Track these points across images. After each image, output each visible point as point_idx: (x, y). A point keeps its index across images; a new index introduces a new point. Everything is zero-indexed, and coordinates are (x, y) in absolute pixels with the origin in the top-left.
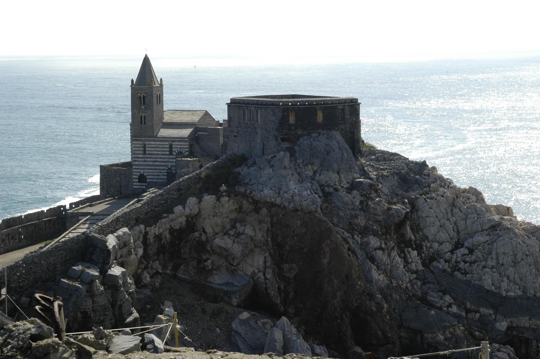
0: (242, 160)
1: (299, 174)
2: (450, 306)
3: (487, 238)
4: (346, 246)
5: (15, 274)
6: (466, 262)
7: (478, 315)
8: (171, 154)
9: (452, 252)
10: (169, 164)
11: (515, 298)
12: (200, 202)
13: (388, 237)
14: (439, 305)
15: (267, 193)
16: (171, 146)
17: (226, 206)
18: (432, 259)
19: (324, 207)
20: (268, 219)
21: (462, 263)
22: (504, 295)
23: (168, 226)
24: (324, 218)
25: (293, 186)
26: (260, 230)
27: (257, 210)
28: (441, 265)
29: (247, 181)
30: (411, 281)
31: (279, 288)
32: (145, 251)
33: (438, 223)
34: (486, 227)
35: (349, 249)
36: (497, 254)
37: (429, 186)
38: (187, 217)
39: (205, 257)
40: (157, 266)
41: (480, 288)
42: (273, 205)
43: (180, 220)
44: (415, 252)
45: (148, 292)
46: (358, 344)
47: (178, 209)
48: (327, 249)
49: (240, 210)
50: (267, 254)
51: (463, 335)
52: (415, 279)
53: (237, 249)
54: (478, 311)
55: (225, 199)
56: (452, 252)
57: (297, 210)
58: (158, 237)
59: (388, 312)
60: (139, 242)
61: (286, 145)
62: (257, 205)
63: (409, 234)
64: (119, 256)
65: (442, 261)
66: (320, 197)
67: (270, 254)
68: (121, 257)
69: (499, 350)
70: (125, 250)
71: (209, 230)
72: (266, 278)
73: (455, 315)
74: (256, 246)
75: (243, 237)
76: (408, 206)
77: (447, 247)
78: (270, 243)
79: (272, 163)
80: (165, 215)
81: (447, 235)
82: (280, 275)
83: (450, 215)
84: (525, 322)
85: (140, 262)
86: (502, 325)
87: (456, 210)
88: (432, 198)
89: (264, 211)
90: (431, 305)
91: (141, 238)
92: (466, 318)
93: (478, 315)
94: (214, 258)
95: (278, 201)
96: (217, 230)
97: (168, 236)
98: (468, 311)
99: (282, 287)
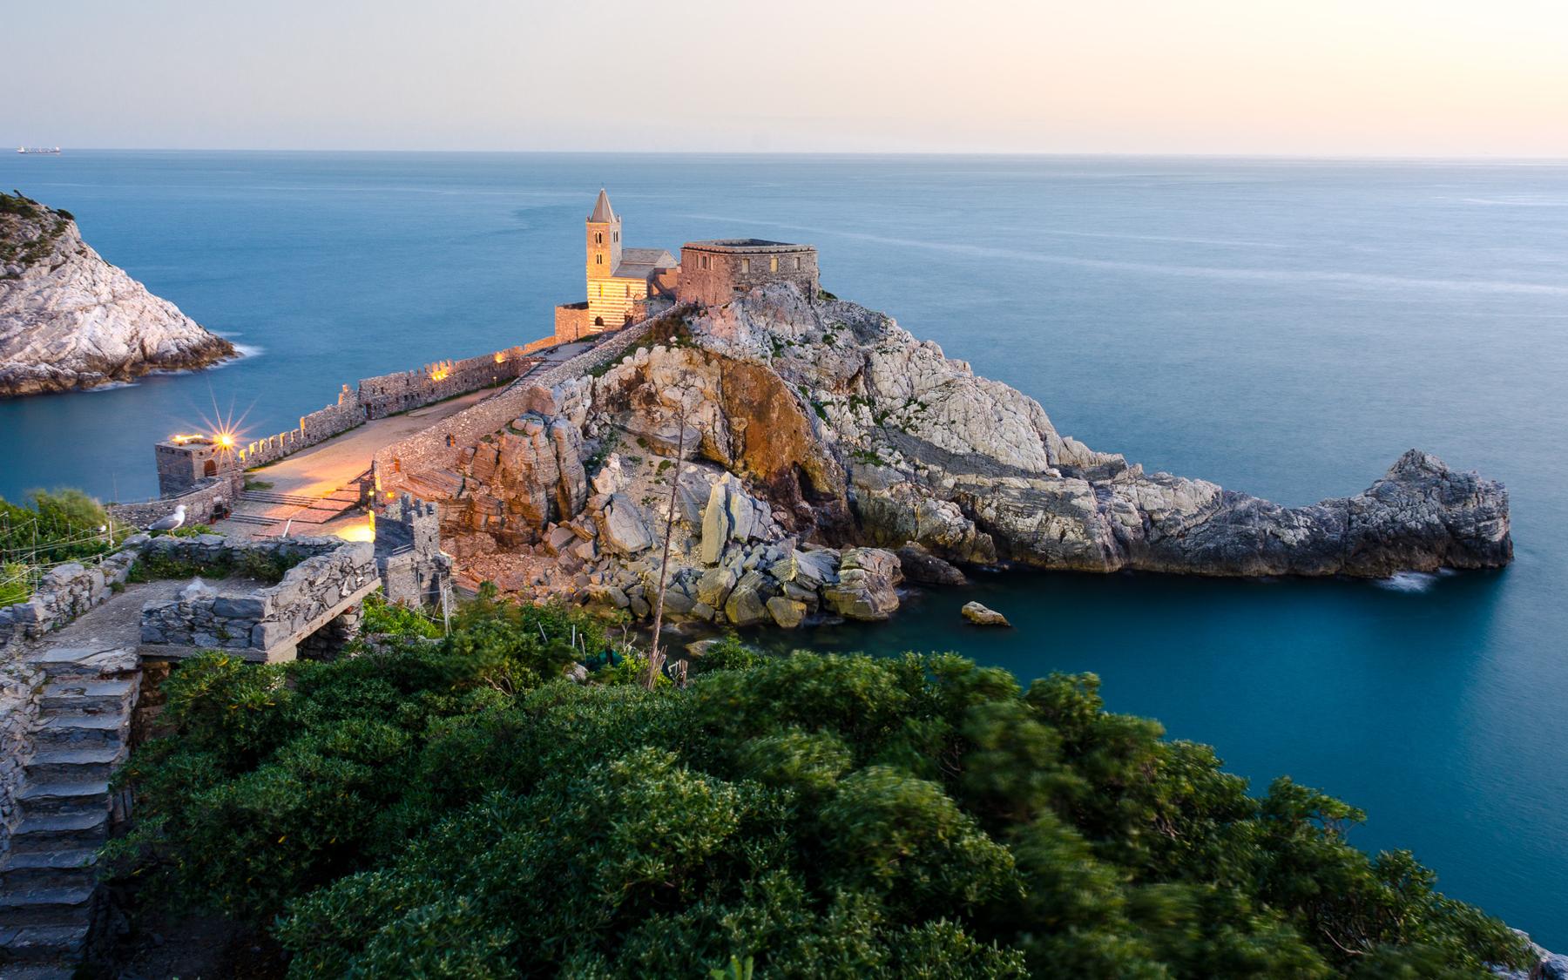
0: (695, 309)
1: (751, 326)
2: (898, 462)
3: (940, 394)
4: (796, 401)
5: (460, 425)
6: (917, 418)
7: (926, 471)
8: (628, 293)
9: (905, 408)
10: (627, 307)
11: (963, 456)
12: (649, 352)
13: (840, 391)
14: (888, 461)
15: (718, 346)
16: (628, 289)
17: (676, 357)
18: (885, 414)
20: (718, 371)
21: (914, 420)
22: (953, 451)
23: (617, 377)
24: (775, 373)
25: (744, 336)
26: (710, 382)
27: (708, 362)
28: (893, 420)
29: (698, 331)
30: (861, 438)
31: (728, 442)
32: (594, 401)
34: (940, 383)
35: (799, 404)
36: (949, 411)
37: (886, 340)
39: (654, 409)
41: (930, 446)
42: (724, 357)
43: (629, 370)
44: (866, 409)
45: (595, 443)
46: (805, 499)
47: (627, 359)
48: (776, 404)
49: (690, 361)
50: (717, 407)
51: (909, 492)
53: (687, 402)
54: (925, 468)
56: (905, 408)
57: (747, 363)
58: (608, 388)
59: (836, 468)
60: (588, 393)
61: (740, 294)
62: (707, 358)
63: (863, 391)
65: (894, 417)
66: (771, 350)
67: (720, 407)
69: (943, 507)
70: (572, 402)
71: (659, 382)
72: (714, 432)
73: (903, 472)
74: (705, 399)
75: (692, 389)
76: (863, 360)
77: (900, 403)
78: (720, 396)
79: (724, 314)
80: (614, 365)
82: (728, 428)
83: (905, 370)
84: (971, 479)
85: (588, 413)
86: (949, 482)
87: (911, 365)
88: (886, 352)
89: (715, 363)
90: (878, 462)
91: (590, 389)
92: (915, 474)
93: (926, 471)
94: (663, 409)
95: (729, 353)
96: (668, 381)
97: (617, 387)
98: (917, 468)
99: (731, 440)
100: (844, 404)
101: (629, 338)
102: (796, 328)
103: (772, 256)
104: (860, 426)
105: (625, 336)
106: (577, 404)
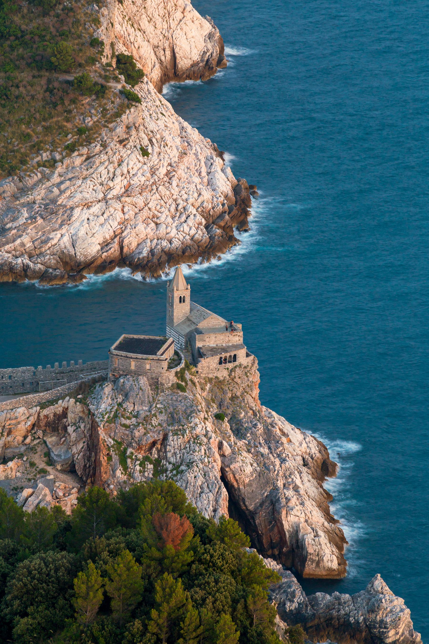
17: (78, 408)
19: (106, 425)
23: (53, 411)
31: (85, 466)
33: (172, 451)
38: (64, 408)
40: (40, 433)
43: (59, 409)
52: (144, 481)
55: (78, 403)
58: (46, 417)
64: (7, 424)
67: (88, 444)
68: (9, 425)
70: (13, 422)
72: (77, 459)
77: (170, 467)
81: (175, 460)
97: (52, 417)
99: (88, 465)
100: (139, 460)
101: (69, 389)
102: (136, 407)
103: (131, 360)
104: (144, 476)
105: (67, 387)
106: (19, 423)
